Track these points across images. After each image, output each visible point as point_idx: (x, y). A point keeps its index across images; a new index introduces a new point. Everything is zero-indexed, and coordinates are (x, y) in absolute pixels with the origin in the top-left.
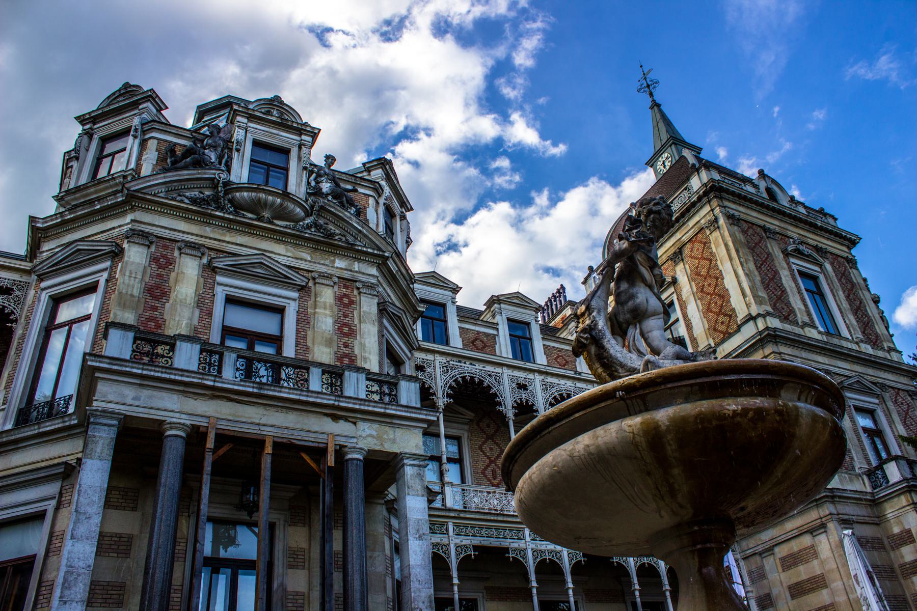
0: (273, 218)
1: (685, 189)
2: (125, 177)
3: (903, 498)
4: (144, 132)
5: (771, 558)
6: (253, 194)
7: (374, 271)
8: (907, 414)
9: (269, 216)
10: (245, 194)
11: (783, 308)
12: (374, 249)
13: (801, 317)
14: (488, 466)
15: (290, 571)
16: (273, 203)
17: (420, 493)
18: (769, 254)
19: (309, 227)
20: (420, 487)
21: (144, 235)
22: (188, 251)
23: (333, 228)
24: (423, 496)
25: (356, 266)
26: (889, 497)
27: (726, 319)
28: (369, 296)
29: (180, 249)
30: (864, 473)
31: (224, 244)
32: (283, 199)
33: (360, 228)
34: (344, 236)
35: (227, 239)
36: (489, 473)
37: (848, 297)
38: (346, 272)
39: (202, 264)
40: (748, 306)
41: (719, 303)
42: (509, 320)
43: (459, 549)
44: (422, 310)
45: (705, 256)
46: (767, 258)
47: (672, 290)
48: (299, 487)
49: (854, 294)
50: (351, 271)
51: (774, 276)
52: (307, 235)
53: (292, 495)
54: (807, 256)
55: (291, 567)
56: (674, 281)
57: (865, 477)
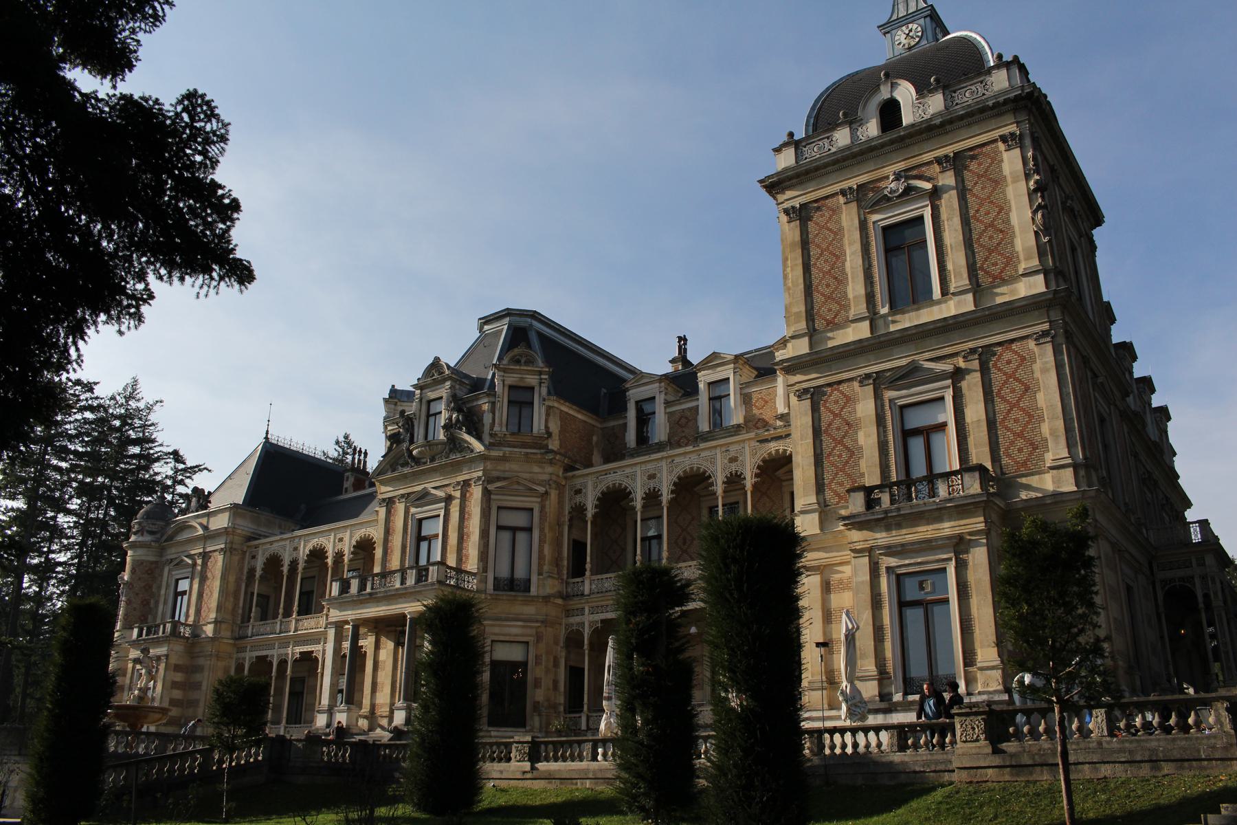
11: (830, 310)
18: (841, 229)
32: (429, 446)
46: (834, 240)
49: (991, 202)
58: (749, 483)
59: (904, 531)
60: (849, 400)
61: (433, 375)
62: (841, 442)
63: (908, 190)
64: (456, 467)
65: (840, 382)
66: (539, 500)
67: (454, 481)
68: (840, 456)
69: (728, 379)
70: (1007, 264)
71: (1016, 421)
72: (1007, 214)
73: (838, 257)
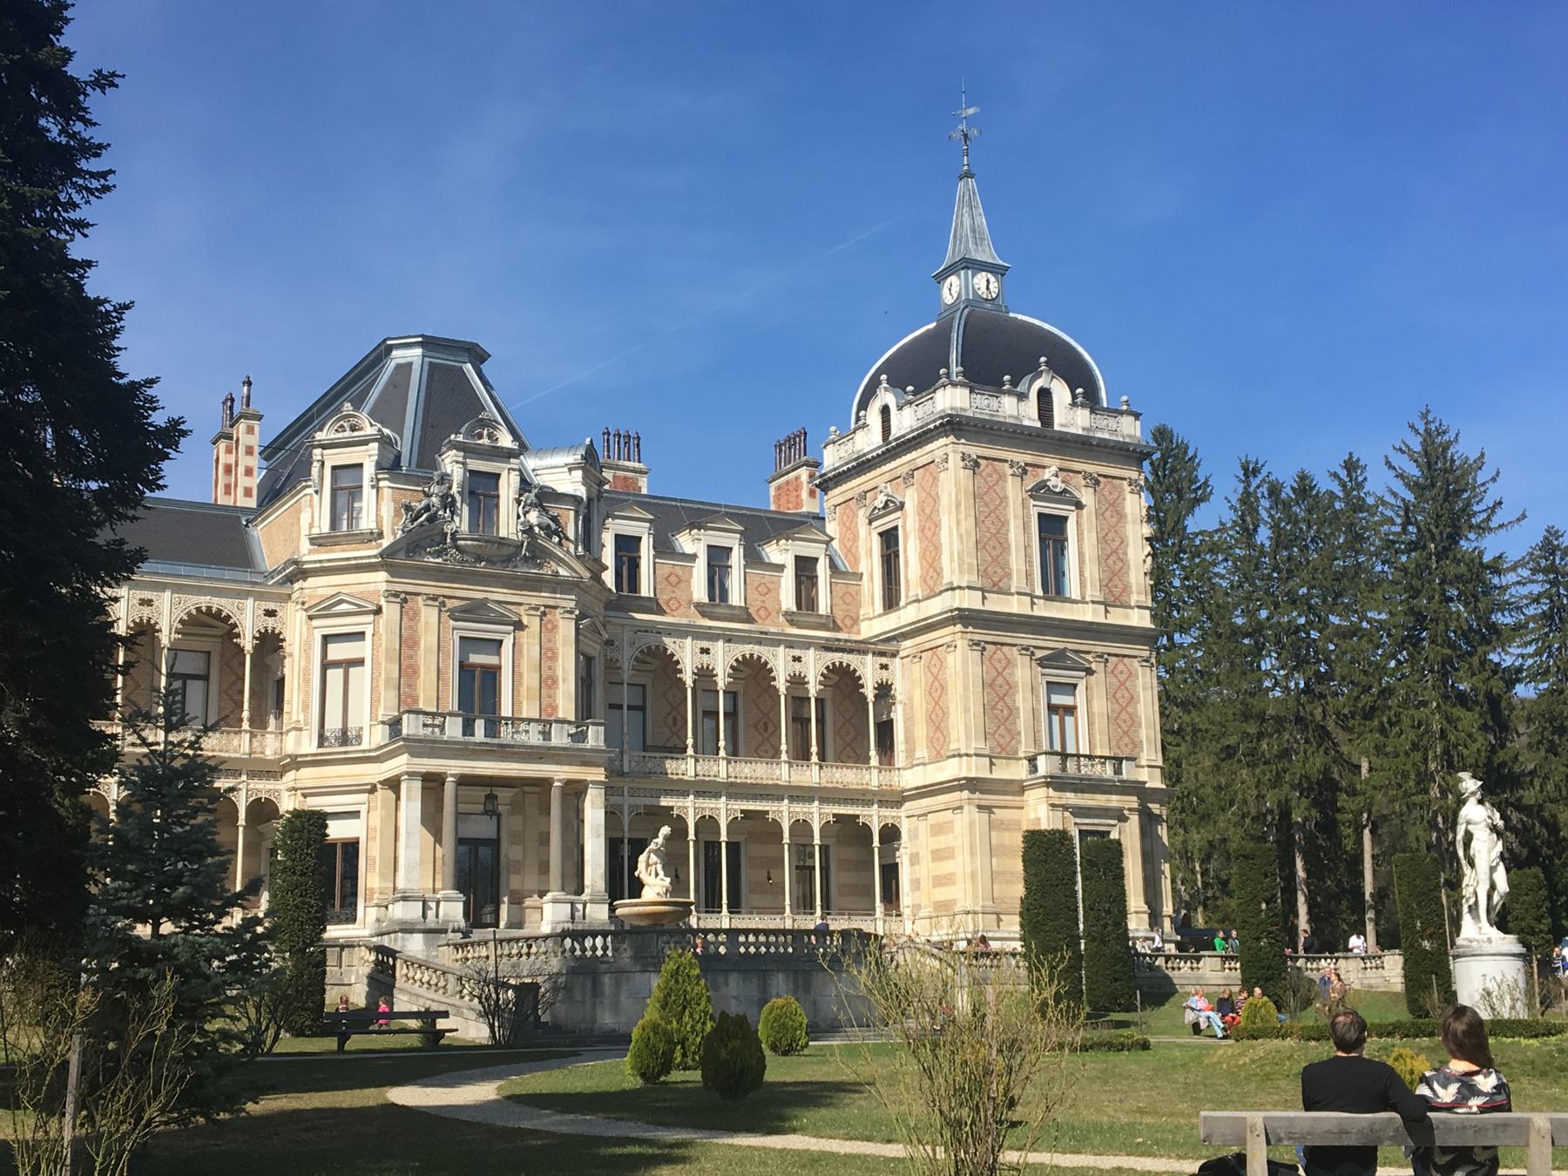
1: (931, 398)
2: (372, 533)
3: (1042, 789)
4: (378, 480)
5: (924, 822)
7: (573, 597)
8: (1122, 684)
10: (469, 542)
11: (996, 573)
13: (1017, 582)
14: (669, 714)
15: (513, 846)
18: (1004, 499)
21: (396, 595)
26: (1033, 787)
27: (935, 574)
30: (1025, 758)
36: (670, 720)
37: (1103, 540)
40: (952, 572)
41: (933, 554)
42: (709, 546)
45: (933, 493)
47: (899, 514)
51: (1000, 529)
54: (1061, 493)
55: (512, 843)
56: (902, 506)
57: (1025, 762)
58: (813, 690)
59: (1086, 795)
60: (1009, 663)
61: (480, 436)
62: (1002, 699)
63: (1065, 491)
64: (535, 584)
65: (1003, 644)
66: (598, 647)
67: (534, 601)
68: (1002, 711)
69: (731, 549)
70: (1124, 591)
71: (1125, 721)
72: (1127, 546)
73: (1003, 524)
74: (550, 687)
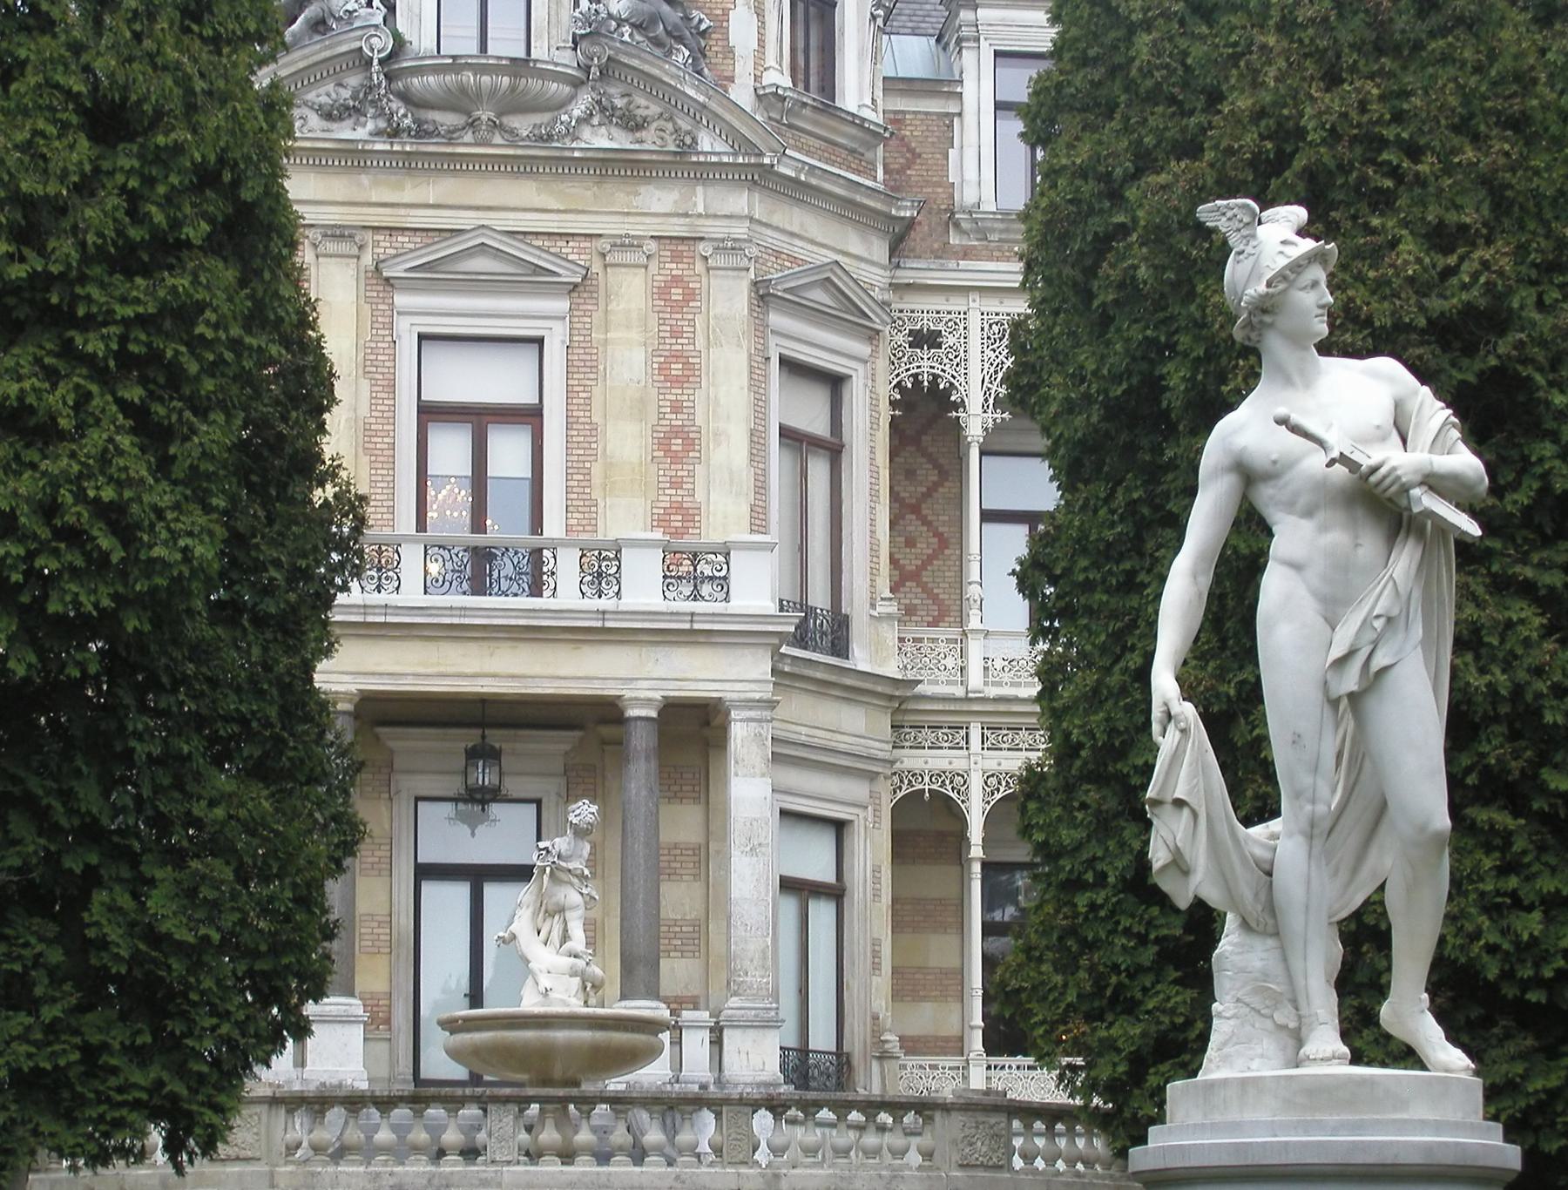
0: (499, 115)
6: (448, 78)
9: (492, 115)
12: (735, 154)
16: (494, 91)
17: (757, 771)
19: (585, 120)
20: (759, 759)
22: (332, 247)
23: (642, 102)
24: (763, 775)
25: (701, 198)
28: (730, 273)
29: (315, 246)
31: (402, 211)
32: (515, 75)
33: (701, 99)
34: (671, 119)
35: (408, 195)
38: (674, 220)
39: (362, 269)
43: (993, 780)
44: (908, 214)
48: (577, 734)
50: (686, 215)
52: (577, 154)
53: (567, 747)
74: (676, 458)
